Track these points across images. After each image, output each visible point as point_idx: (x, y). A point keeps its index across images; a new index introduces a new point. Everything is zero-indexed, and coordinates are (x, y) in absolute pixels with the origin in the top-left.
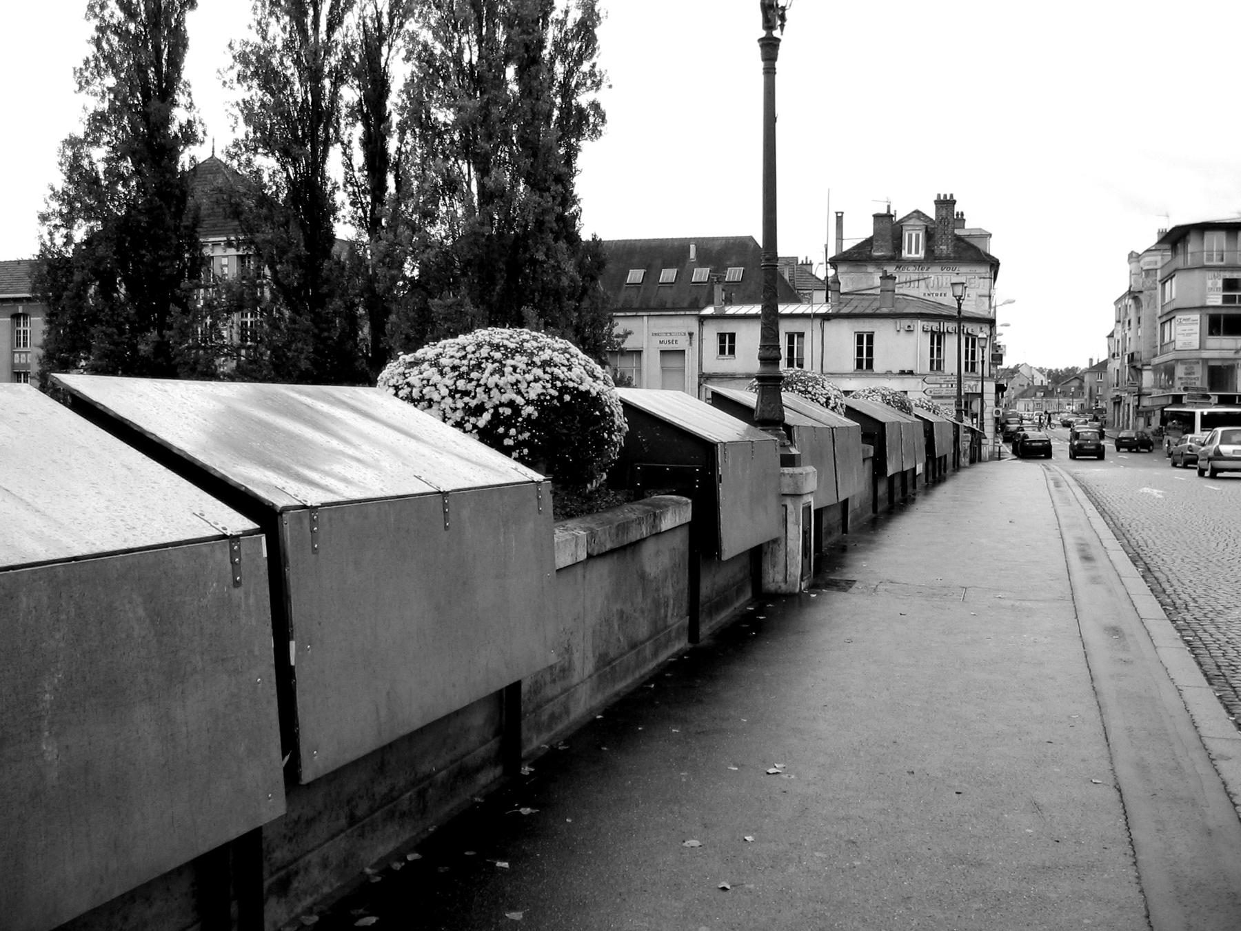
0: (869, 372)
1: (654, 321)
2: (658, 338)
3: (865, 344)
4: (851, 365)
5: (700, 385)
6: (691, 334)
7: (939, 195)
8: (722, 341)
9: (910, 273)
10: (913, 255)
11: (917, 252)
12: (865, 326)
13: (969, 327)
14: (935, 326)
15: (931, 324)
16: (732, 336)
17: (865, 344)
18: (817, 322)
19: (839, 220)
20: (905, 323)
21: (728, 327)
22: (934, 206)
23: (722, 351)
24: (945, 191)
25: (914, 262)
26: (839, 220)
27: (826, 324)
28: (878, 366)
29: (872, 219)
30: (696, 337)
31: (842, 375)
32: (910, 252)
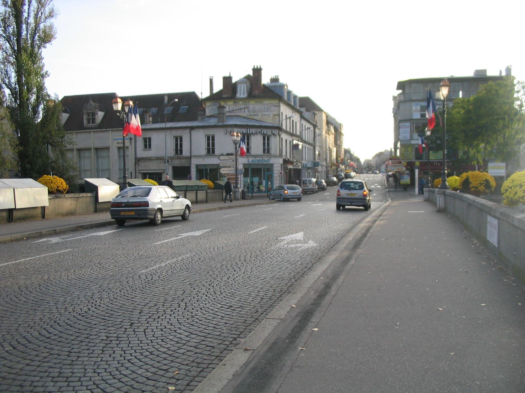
0: (213, 154)
1: (114, 133)
2: (116, 142)
3: (211, 142)
4: (204, 152)
5: (135, 164)
6: (131, 139)
7: (254, 67)
8: (145, 142)
9: (241, 105)
10: (242, 96)
11: (244, 94)
12: (210, 132)
13: (265, 131)
14: (244, 131)
15: (242, 129)
16: (150, 139)
17: (211, 142)
18: (188, 131)
19: (211, 81)
20: (229, 129)
21: (148, 135)
22: (252, 71)
23: (146, 146)
24: (257, 65)
25: (241, 99)
26: (211, 81)
27: (193, 132)
28: (217, 152)
29: (222, 79)
30: (133, 140)
31: (199, 156)
32: (240, 95)
